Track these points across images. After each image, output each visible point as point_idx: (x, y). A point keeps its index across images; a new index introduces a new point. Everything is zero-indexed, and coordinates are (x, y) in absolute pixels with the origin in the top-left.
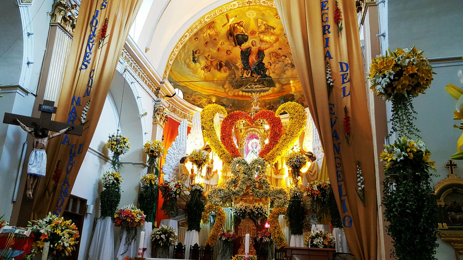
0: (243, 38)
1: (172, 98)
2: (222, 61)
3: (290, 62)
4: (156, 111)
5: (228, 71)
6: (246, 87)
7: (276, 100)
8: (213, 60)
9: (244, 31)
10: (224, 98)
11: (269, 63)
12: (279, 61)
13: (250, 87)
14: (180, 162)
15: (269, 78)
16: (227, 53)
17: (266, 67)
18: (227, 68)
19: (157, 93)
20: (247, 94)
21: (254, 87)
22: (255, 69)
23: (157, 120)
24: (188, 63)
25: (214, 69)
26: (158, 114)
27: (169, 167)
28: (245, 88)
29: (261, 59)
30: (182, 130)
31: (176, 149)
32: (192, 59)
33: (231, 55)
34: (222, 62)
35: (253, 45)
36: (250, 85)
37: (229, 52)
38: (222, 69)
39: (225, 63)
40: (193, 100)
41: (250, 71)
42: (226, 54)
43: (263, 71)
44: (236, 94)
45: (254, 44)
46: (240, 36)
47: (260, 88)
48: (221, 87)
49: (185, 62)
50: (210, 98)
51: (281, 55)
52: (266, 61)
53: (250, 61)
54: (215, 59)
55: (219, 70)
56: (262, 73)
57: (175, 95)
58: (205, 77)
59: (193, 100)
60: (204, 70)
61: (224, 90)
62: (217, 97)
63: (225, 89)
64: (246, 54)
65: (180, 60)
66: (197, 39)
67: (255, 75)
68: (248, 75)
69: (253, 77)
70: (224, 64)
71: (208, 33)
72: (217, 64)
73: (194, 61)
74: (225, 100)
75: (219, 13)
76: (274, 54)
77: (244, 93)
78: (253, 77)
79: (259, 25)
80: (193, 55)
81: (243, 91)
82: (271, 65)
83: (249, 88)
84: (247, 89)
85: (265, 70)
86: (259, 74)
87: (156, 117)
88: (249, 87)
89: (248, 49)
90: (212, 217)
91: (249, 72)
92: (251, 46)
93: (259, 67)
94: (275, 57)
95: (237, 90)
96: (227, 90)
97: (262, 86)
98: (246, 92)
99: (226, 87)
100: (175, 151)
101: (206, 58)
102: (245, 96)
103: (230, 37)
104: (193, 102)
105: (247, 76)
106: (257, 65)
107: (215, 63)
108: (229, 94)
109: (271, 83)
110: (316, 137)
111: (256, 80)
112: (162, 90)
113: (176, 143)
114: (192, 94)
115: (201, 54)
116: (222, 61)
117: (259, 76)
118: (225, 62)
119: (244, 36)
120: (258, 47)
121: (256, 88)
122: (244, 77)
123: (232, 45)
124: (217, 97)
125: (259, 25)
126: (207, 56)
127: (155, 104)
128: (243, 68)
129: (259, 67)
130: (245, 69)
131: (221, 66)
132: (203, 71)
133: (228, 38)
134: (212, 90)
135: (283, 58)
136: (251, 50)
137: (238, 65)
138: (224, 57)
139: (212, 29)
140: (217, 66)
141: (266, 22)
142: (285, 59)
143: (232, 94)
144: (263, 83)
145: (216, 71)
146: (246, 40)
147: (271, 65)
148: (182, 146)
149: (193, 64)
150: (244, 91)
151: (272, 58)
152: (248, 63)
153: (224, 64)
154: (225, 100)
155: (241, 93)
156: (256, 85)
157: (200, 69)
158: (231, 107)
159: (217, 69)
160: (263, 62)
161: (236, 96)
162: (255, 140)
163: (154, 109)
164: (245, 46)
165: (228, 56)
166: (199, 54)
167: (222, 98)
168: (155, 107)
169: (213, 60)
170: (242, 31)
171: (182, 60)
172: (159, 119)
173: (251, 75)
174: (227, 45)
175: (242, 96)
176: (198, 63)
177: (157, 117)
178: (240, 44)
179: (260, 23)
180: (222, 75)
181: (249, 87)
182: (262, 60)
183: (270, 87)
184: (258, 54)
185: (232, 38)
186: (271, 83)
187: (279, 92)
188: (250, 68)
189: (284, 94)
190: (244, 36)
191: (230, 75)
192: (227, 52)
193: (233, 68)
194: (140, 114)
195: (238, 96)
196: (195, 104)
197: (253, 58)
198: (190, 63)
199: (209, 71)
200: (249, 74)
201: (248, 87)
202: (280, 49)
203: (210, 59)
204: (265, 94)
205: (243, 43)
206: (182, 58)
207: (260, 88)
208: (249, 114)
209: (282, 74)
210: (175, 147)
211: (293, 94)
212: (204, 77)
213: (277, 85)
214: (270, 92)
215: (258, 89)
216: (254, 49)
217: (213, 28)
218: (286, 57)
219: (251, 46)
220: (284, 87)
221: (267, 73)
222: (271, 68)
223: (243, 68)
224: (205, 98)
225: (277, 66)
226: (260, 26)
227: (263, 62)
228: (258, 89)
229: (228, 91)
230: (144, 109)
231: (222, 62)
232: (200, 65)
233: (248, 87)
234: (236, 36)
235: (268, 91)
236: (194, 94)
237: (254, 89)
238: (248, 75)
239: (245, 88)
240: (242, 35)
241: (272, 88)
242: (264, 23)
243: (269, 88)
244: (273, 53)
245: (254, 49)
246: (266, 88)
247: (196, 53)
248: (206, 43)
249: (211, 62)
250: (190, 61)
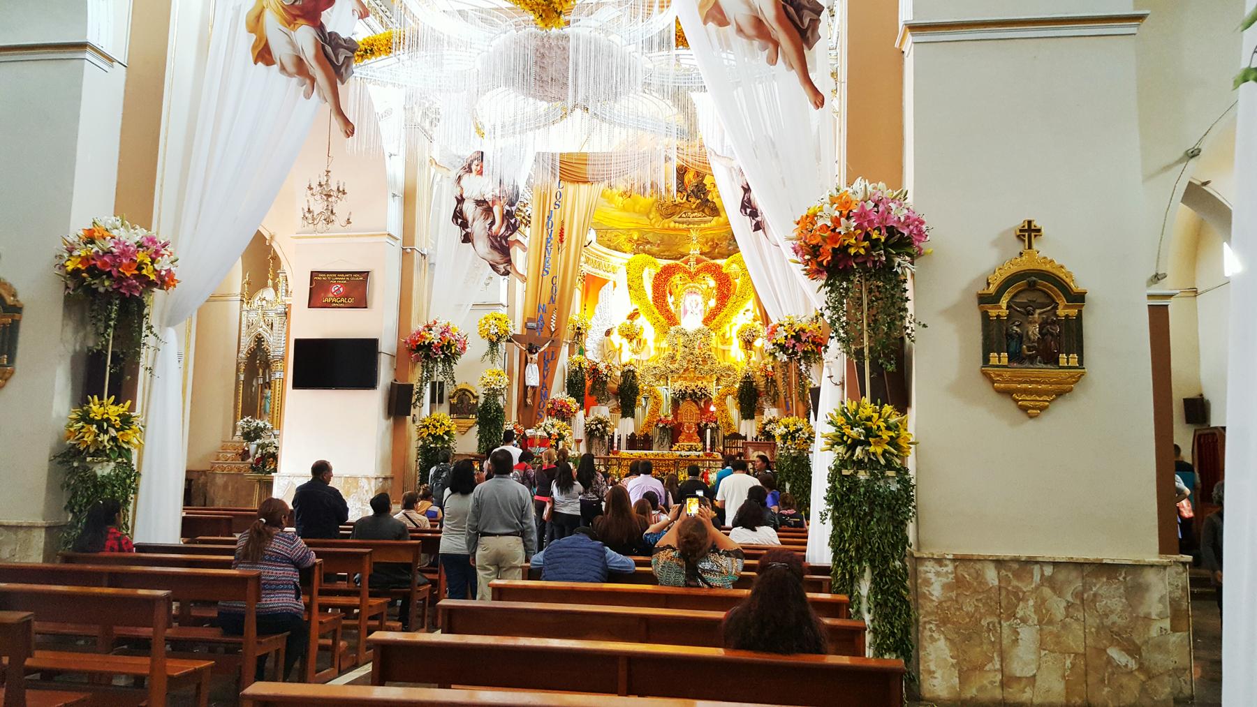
20: (681, 226)
22: (692, 191)
44: (666, 225)
48: (645, 217)
53: (686, 180)
67: (693, 200)
74: (651, 234)
77: (677, 224)
85: (706, 193)
86: (698, 198)
90: (643, 399)
96: (653, 221)
98: (679, 223)
99: (651, 216)
105: (681, 201)
111: (694, 206)
132: (621, 198)
144: (703, 211)
154: (651, 234)
155: (672, 225)
158: (659, 245)
167: (647, 233)
173: (687, 199)
175: (675, 229)
181: (684, 215)
182: (702, 180)
188: (685, 190)
195: (669, 228)
197: (689, 177)
200: (685, 198)
204: (706, 225)
210: (599, 317)
214: (713, 223)
221: (709, 197)
241: (716, 218)
246: (708, 218)
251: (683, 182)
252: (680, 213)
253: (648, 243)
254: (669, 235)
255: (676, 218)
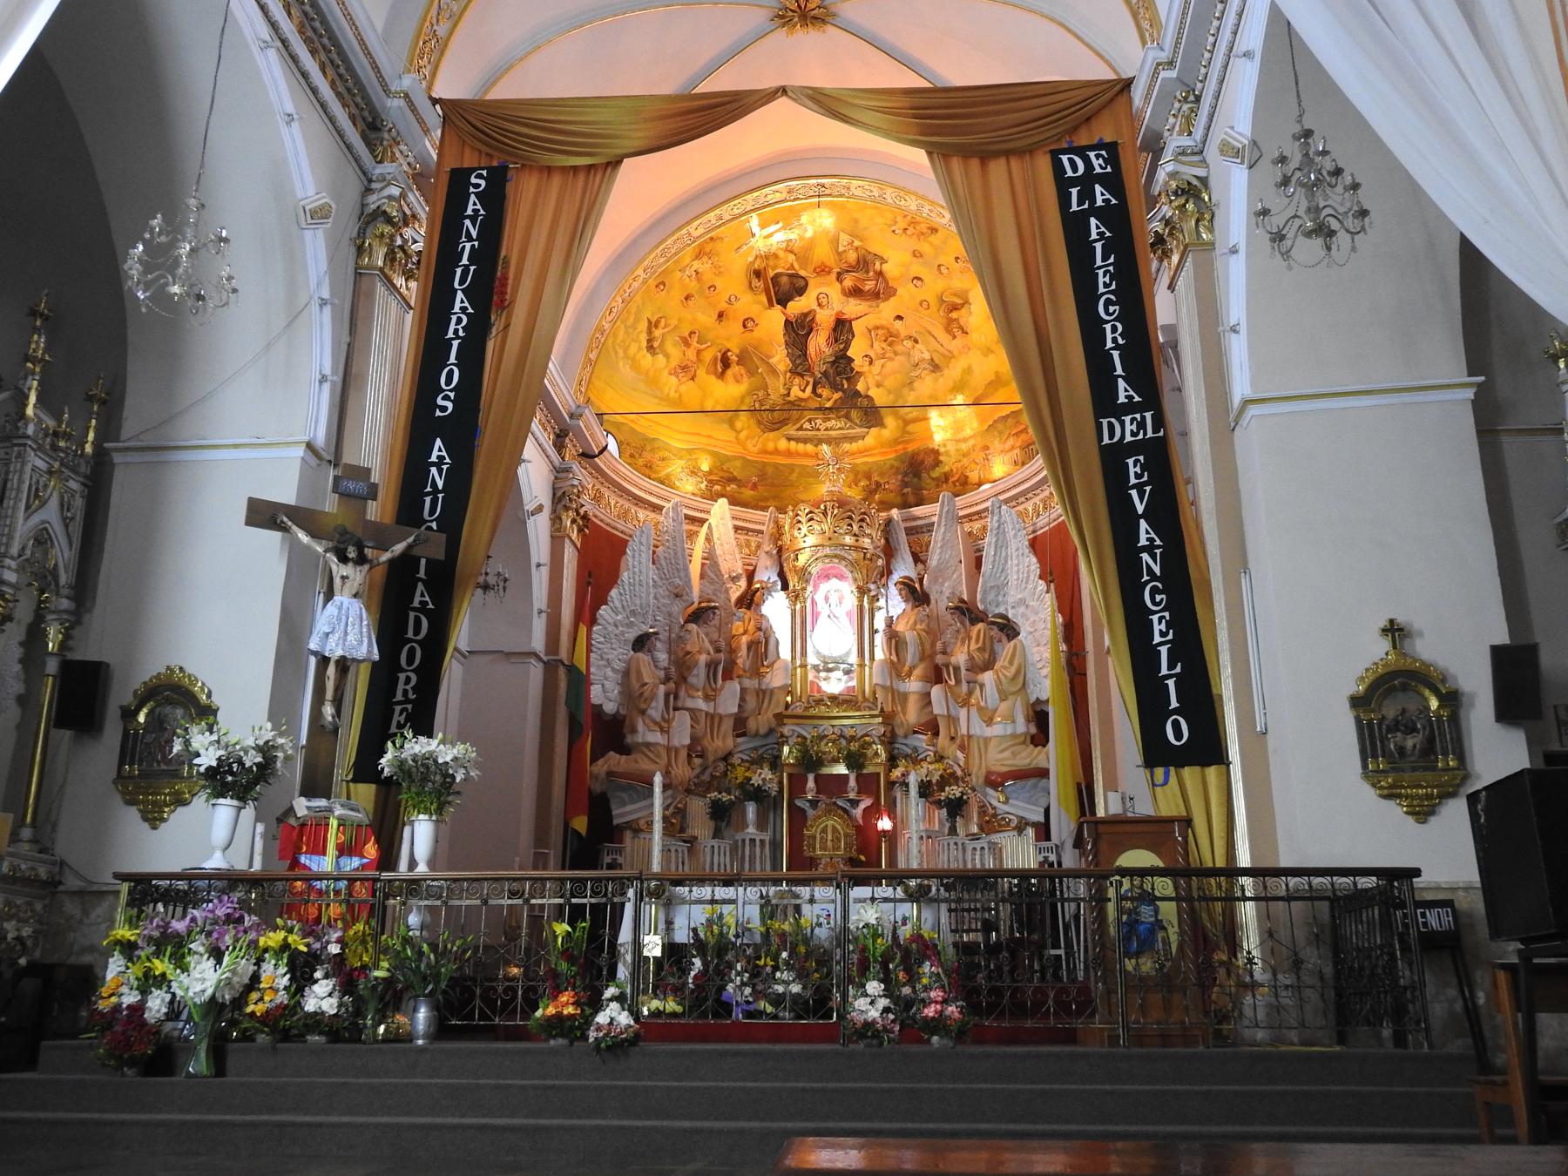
0: (793, 284)
1: (596, 459)
2: (729, 350)
3: (927, 356)
4: (560, 500)
5: (745, 379)
6: (798, 426)
7: (888, 466)
8: (704, 346)
9: (796, 266)
10: (736, 458)
11: (866, 356)
12: (896, 353)
13: (809, 427)
14: (633, 650)
15: (865, 403)
16: (745, 326)
17: (857, 369)
18: (743, 371)
19: (559, 445)
20: (801, 447)
21: (822, 427)
22: (825, 374)
23: (564, 523)
24: (634, 355)
25: (708, 372)
26: (567, 508)
27: (601, 663)
28: (798, 430)
29: (842, 346)
30: (637, 555)
31: (621, 610)
32: (644, 344)
33: (757, 333)
34: (729, 354)
35: (819, 305)
36: (810, 421)
37: (750, 324)
38: (729, 372)
39: (737, 356)
40: (646, 466)
41: (811, 380)
42: (742, 329)
43: (848, 379)
44: (770, 446)
45: (824, 301)
46: (784, 280)
47: (840, 429)
48: (726, 426)
49: (625, 351)
50: (694, 457)
51: (902, 336)
52: (857, 350)
53: (811, 350)
54: (709, 344)
55: (721, 376)
56: (846, 386)
57: (605, 453)
58: (680, 396)
59: (646, 466)
60: (677, 377)
61: (734, 434)
62: (715, 455)
63: (738, 432)
64: (799, 330)
65: (614, 348)
66: (662, 287)
67: (825, 392)
68: (804, 391)
69: (820, 396)
70: (734, 358)
71: (694, 268)
72: (715, 359)
73: (650, 348)
75: (731, 213)
76: (880, 332)
77: (793, 444)
78: (820, 396)
79: (841, 249)
80: (650, 332)
81: (789, 439)
82: (871, 363)
83: (806, 429)
84: (801, 432)
85: (853, 377)
86: (835, 387)
87: (560, 519)
88: (807, 425)
89: (805, 315)
91: (807, 385)
92: (815, 306)
93: (837, 367)
94: (885, 341)
95: (772, 435)
96: (743, 435)
97: (846, 424)
98: (798, 440)
99: (739, 425)
100: (619, 618)
101: (686, 343)
102: (798, 454)
103: (755, 282)
104: (647, 471)
105: (801, 395)
106: (833, 363)
107: (708, 356)
108: (750, 445)
109: (872, 415)
110: (1018, 571)
112: (572, 438)
113: (621, 594)
114: (643, 449)
115: (672, 327)
116: (729, 350)
117: (837, 396)
118: (737, 351)
119: (795, 281)
120: (835, 312)
121: (826, 429)
122: (792, 394)
123: (760, 303)
124: (715, 455)
125: (841, 249)
126: (686, 334)
127: (556, 478)
128: (790, 371)
129: (837, 367)
130: (794, 372)
131: (726, 363)
132: (674, 380)
133: (750, 283)
134: (699, 434)
135: (909, 344)
136: (814, 316)
137: (773, 361)
138: (732, 338)
139: (705, 259)
140: (716, 365)
141: (861, 241)
142: (913, 347)
143: (759, 445)
144: (847, 417)
145: (713, 378)
146: (801, 291)
147: (871, 363)
148: (638, 602)
149: (646, 360)
150: (793, 439)
151: (876, 345)
152: (805, 355)
153: (734, 358)
154: (738, 463)
155: (783, 444)
156: (829, 419)
157: (666, 373)
158: (754, 487)
159: (715, 373)
160: (849, 353)
161: (771, 453)
162: (834, 582)
163: (554, 494)
164: (797, 306)
165: (748, 335)
166: (666, 330)
167: (729, 459)
168: (557, 486)
169: (704, 346)
170: (792, 265)
171: (617, 347)
172: (569, 523)
173: (814, 391)
174: (751, 303)
175: (788, 453)
176: (660, 356)
177: (564, 517)
178: (783, 302)
179: (845, 243)
180: (729, 390)
181: (807, 425)
182: (847, 348)
183: (870, 428)
184: (834, 330)
185: (761, 284)
186: (872, 415)
187: (896, 442)
189: (911, 448)
190: (795, 281)
191: (750, 392)
192: (744, 323)
193: (760, 371)
194: (526, 508)
195: (776, 452)
196: (653, 476)
197: (819, 344)
198: (639, 356)
199: (693, 379)
200: (809, 389)
201: (804, 426)
202: (899, 318)
203: (695, 343)
204: (854, 446)
205: (790, 298)
206: (618, 341)
207: (840, 429)
208: (819, 508)
209: (905, 391)
210: (617, 604)
211: (937, 447)
212: (677, 395)
213: (890, 421)
215: (833, 433)
216: (825, 318)
217: (710, 255)
218: (916, 341)
219: (815, 306)
220: (910, 428)
221: (860, 387)
222: (870, 372)
223: (790, 371)
224: (681, 458)
225: (889, 365)
226: (845, 251)
227: (849, 353)
228: (833, 433)
229: (747, 438)
230: (534, 495)
231: (729, 354)
232: (668, 361)
233: (804, 426)
234: (772, 279)
235: (863, 438)
236: (648, 448)
237: (822, 432)
238: (804, 391)
239: (798, 430)
240: (790, 276)
242: (857, 243)
243: (866, 430)
244: (877, 328)
245: (825, 318)
246: (859, 430)
247: (656, 326)
248: (687, 298)
249: (699, 352)
250: (640, 349)
251: (805, 354)
252: (798, 420)
253: (732, 480)
254: (776, 466)
255: (791, 430)
